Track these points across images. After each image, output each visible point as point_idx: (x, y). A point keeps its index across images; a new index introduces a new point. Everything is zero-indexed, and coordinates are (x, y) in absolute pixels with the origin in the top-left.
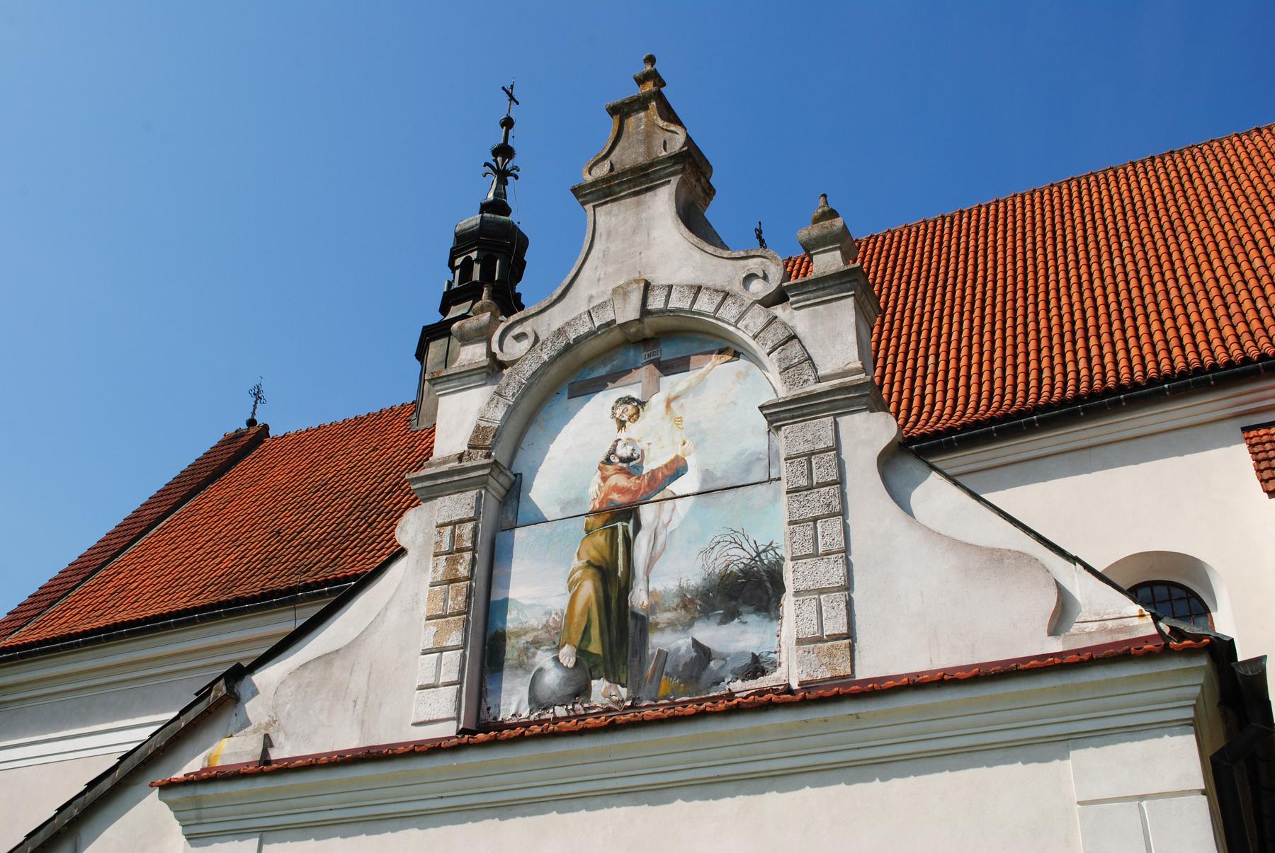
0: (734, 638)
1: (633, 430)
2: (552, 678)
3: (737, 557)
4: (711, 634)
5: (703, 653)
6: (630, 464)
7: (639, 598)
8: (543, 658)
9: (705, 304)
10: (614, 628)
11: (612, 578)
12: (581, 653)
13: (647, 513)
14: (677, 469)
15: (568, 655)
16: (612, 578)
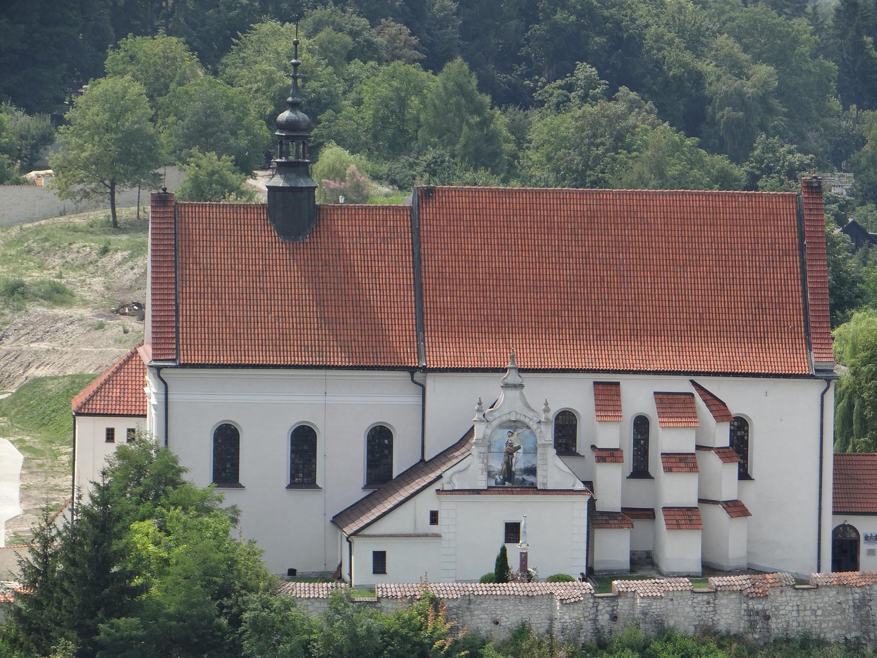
0: (530, 479)
1: (512, 438)
2: (499, 480)
3: (529, 465)
4: (525, 477)
5: (524, 480)
6: (511, 445)
7: (513, 469)
8: (497, 477)
9: (527, 420)
10: (508, 473)
11: (508, 465)
12: (504, 477)
13: (515, 454)
14: (519, 448)
15: (501, 477)
16: (508, 465)
